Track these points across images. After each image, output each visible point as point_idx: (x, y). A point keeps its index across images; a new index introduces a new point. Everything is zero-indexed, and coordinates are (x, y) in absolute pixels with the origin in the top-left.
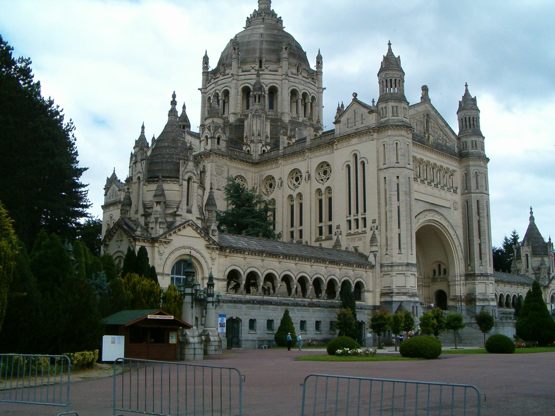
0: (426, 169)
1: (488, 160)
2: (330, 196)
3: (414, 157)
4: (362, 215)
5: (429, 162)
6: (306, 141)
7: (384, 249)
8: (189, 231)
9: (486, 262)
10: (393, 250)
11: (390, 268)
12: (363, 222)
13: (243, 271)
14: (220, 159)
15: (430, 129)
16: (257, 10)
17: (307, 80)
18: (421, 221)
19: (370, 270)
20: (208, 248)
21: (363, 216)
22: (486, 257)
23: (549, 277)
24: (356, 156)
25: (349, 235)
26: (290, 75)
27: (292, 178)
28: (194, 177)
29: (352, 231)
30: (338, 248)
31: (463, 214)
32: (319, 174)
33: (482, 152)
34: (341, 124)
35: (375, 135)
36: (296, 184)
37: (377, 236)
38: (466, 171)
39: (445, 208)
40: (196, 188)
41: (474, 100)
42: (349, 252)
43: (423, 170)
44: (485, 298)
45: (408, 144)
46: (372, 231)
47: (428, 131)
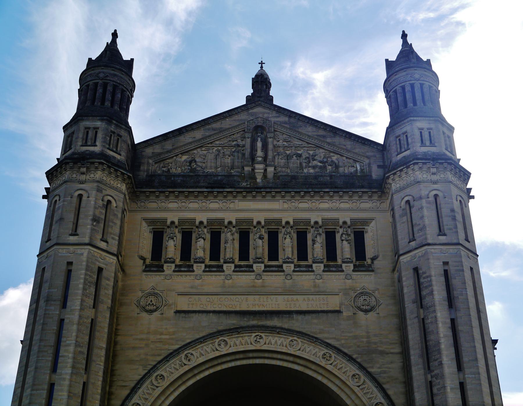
39: (308, 317)
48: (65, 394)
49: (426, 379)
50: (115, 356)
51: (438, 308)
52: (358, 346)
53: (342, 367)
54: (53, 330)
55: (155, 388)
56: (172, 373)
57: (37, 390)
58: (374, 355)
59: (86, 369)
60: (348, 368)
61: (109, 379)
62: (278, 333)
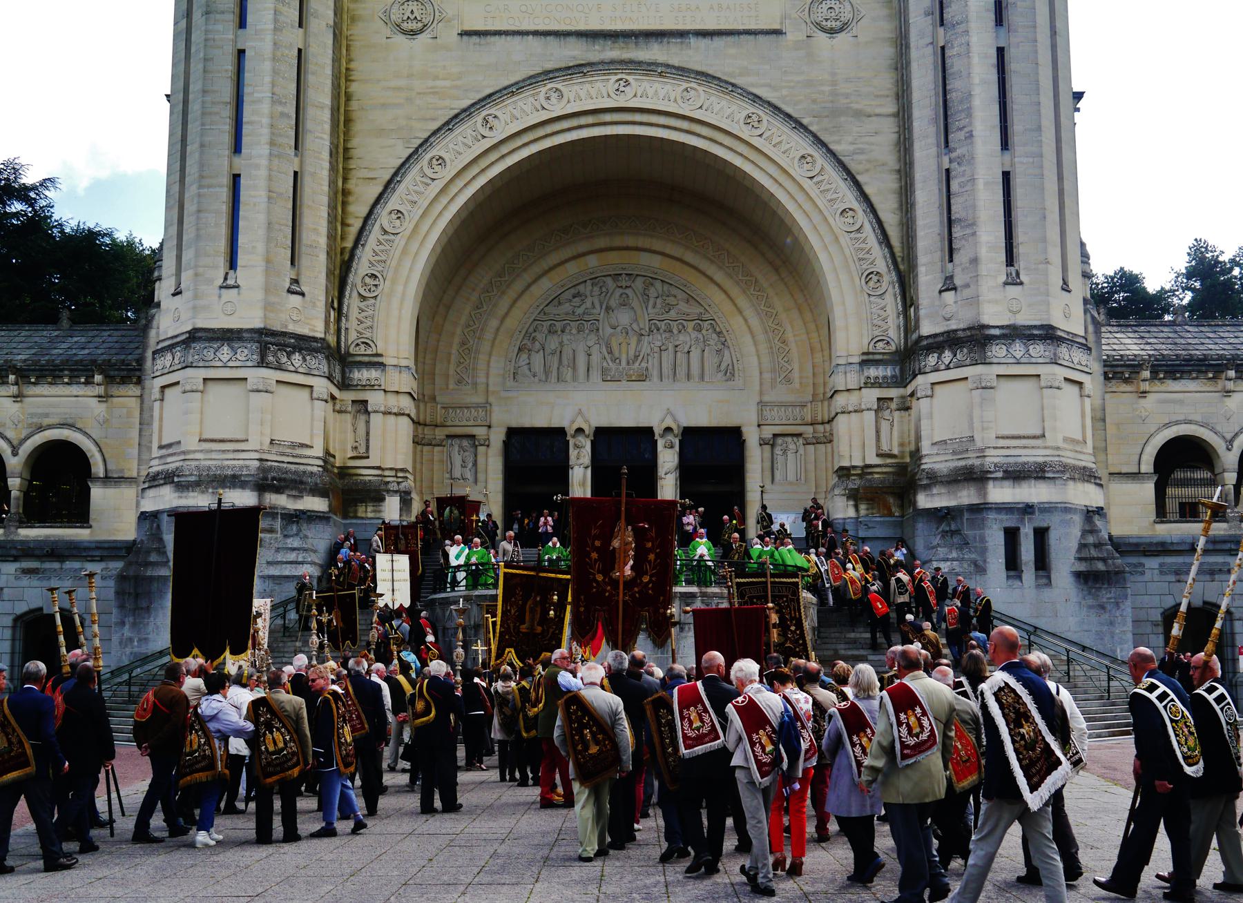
9: (975, 261)
22: (974, 234)
39: (718, 42)
44: (962, 463)
48: (263, 194)
49: (939, 166)
50: (348, 121)
51: (974, 26)
52: (814, 101)
53: (781, 142)
54: (226, 71)
55: (430, 181)
56: (460, 154)
57: (209, 187)
58: (843, 119)
59: (296, 148)
60: (793, 144)
61: (341, 166)
62: (660, 75)
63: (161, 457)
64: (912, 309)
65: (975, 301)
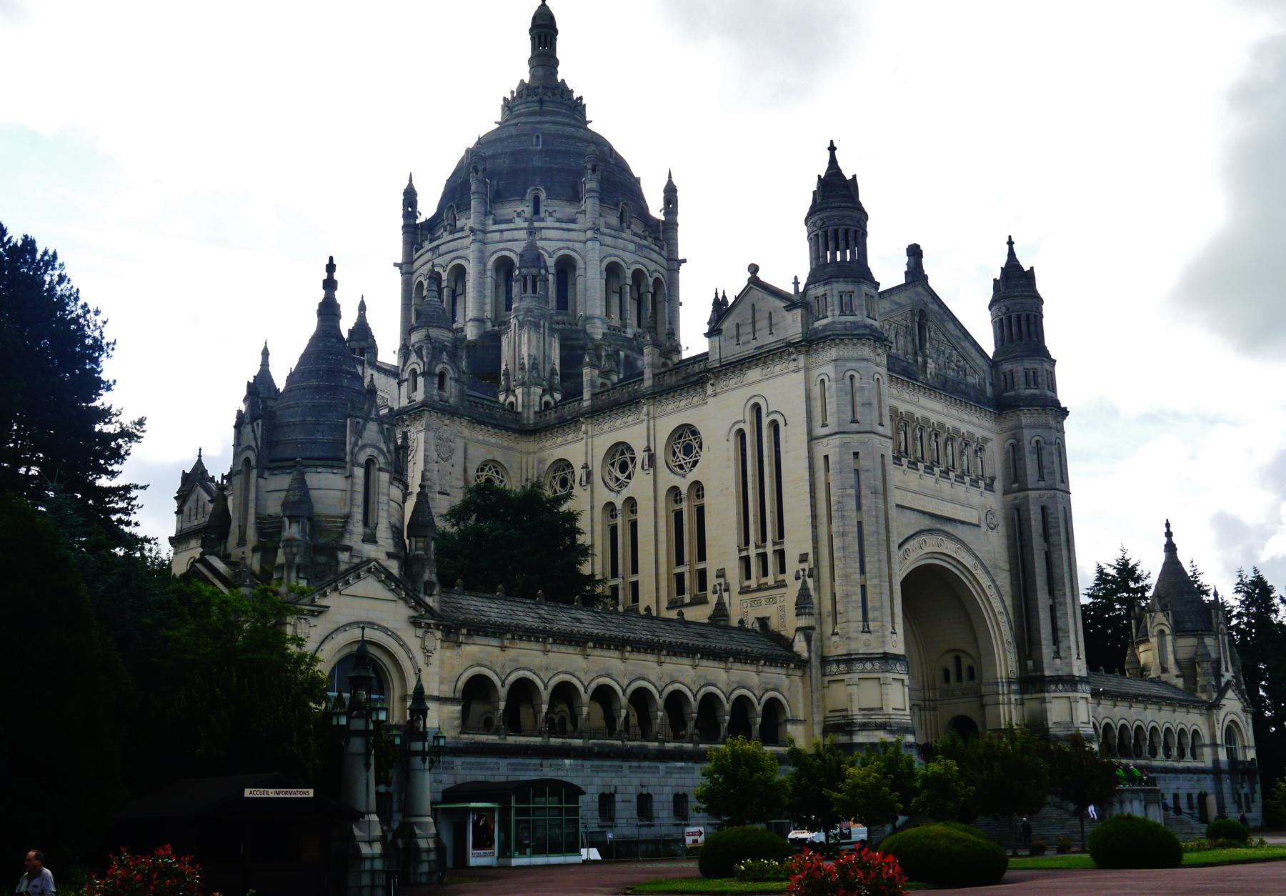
0: (921, 437)
1: (1065, 412)
2: (698, 502)
3: (895, 413)
4: (775, 544)
5: (927, 420)
6: (642, 380)
7: (830, 620)
8: (370, 586)
9: (1069, 648)
10: (851, 624)
11: (844, 666)
12: (778, 560)
13: (500, 678)
14: (447, 422)
15: (928, 345)
16: (527, 81)
17: (645, 242)
18: (912, 557)
19: (799, 673)
20: (415, 622)
21: (777, 548)
22: (1069, 636)
23: (1218, 682)
24: (757, 409)
25: (745, 591)
26: (603, 230)
27: (613, 465)
28: (381, 459)
29: (753, 583)
30: (722, 623)
31: (1008, 540)
32: (674, 453)
33: (1049, 393)
34: (722, 338)
35: (802, 360)
36: (622, 477)
37: (812, 592)
38: (1015, 438)
39: (966, 527)
40: (386, 484)
41: (1030, 275)
42: (748, 630)
43: (915, 439)
45: (878, 379)
46: (800, 582)
47: (922, 347)
63: (864, 715)
64: (1030, 663)
65: (1070, 664)
